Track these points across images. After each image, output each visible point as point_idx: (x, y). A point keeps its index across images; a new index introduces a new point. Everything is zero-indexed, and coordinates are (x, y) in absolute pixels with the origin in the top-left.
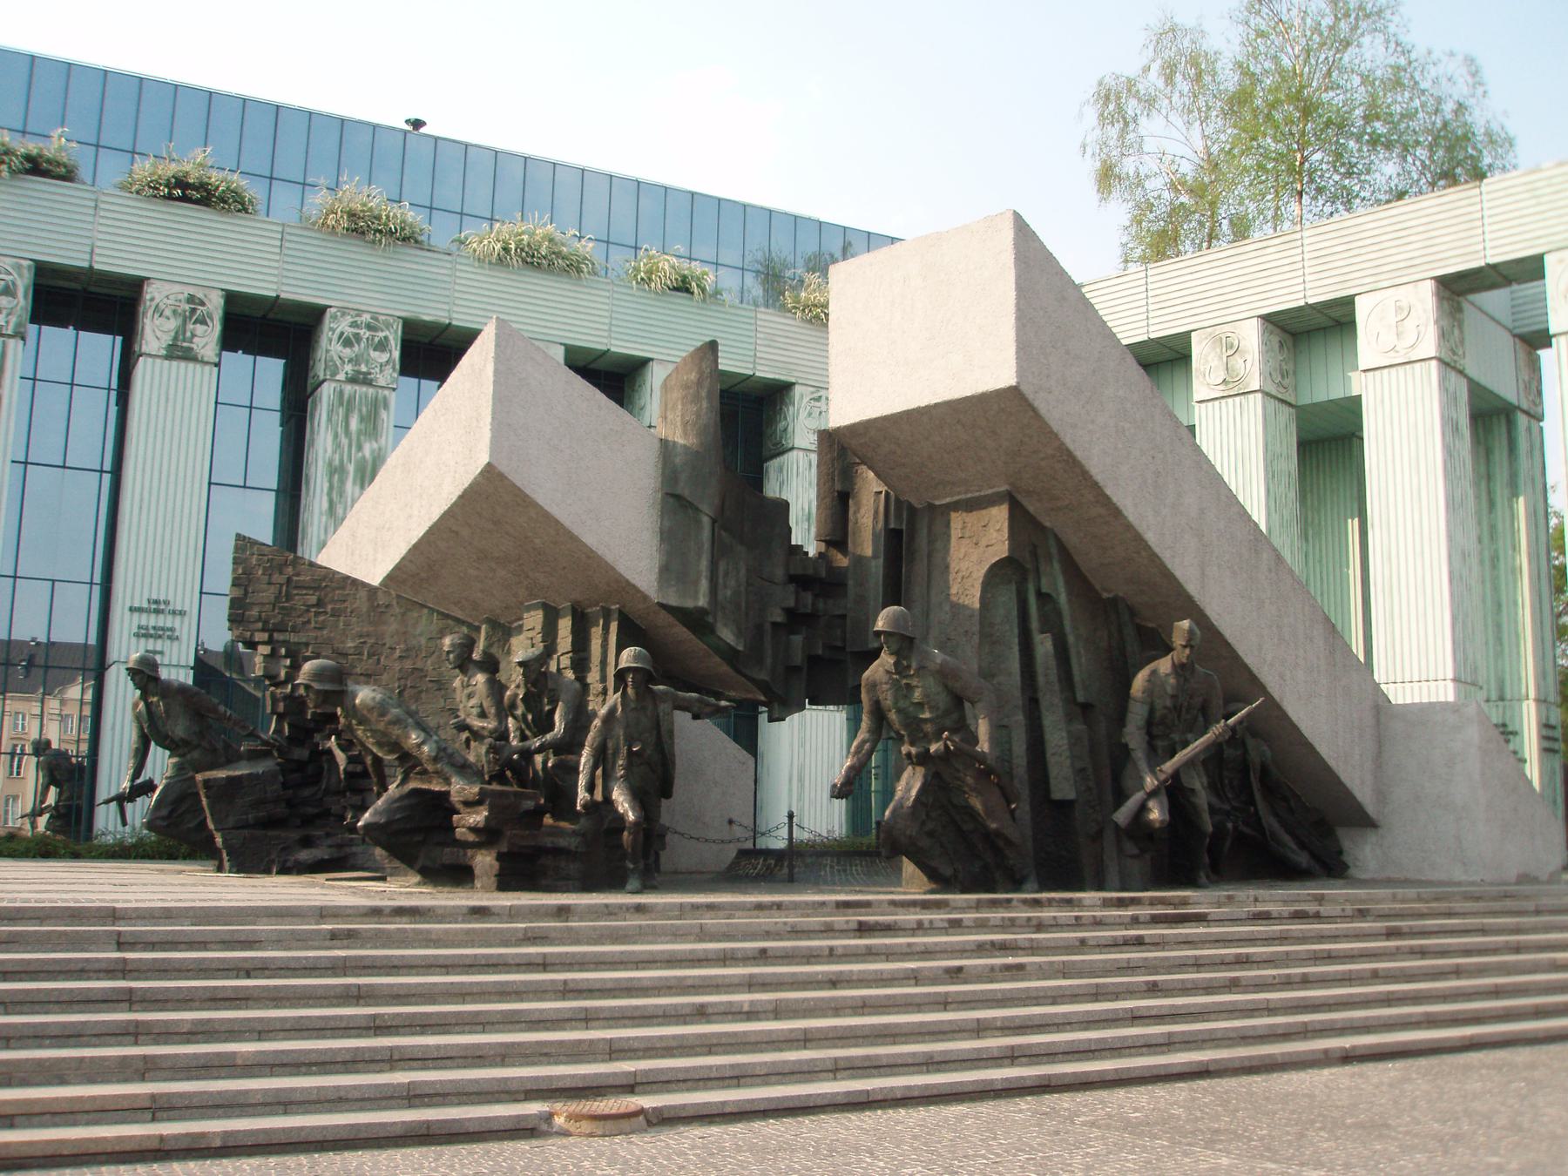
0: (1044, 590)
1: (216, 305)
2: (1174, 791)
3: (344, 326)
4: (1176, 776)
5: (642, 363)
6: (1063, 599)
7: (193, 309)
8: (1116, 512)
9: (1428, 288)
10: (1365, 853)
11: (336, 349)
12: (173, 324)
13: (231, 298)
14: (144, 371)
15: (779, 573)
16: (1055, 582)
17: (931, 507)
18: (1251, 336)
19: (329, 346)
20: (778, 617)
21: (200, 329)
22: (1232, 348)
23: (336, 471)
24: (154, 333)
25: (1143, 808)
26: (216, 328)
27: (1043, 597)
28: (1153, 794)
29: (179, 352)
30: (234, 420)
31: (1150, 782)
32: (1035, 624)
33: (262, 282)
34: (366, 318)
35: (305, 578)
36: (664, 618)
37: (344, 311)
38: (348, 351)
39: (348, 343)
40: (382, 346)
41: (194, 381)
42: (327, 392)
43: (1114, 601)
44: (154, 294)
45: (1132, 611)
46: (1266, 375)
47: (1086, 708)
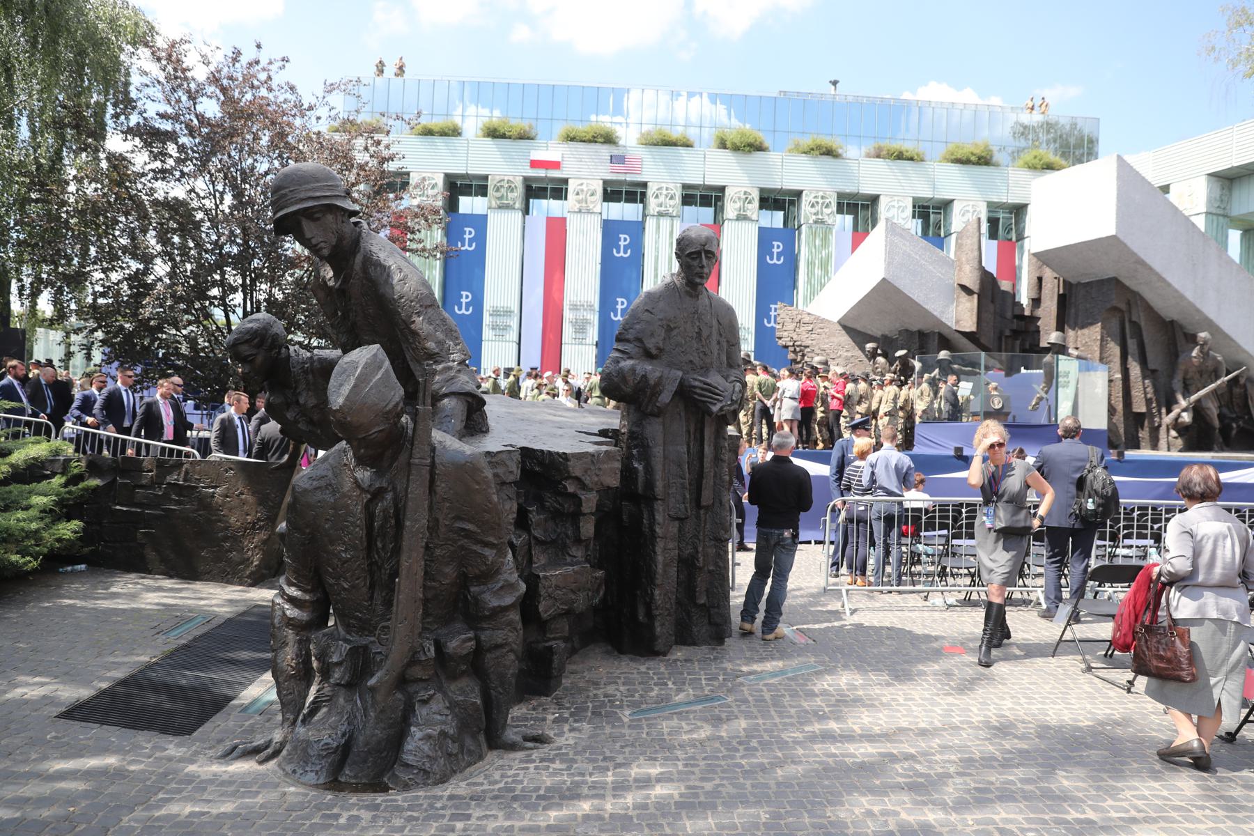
0: (1134, 319)
1: (756, 195)
2: (1197, 409)
3: (811, 198)
4: (1199, 401)
5: (952, 201)
6: (1143, 324)
8: (1169, 285)
11: (809, 209)
13: (762, 190)
15: (1009, 315)
17: (1079, 284)
19: (806, 210)
20: (1008, 333)
21: (750, 206)
23: (810, 264)
24: (730, 210)
25: (1179, 416)
26: (756, 203)
27: (1130, 321)
28: (1184, 410)
29: (742, 218)
31: (1183, 403)
32: (1128, 336)
34: (821, 194)
35: (807, 319)
36: (958, 335)
37: (811, 191)
38: (813, 210)
39: (813, 206)
43: (1172, 322)
45: (1181, 327)
47: (1153, 371)
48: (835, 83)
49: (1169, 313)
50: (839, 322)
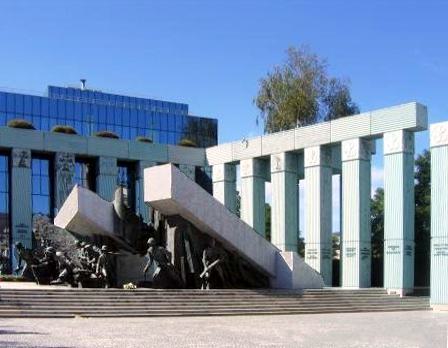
1: (29, 152)
4: (213, 267)
7: (24, 155)
9: (318, 148)
10: (273, 283)
12: (19, 160)
14: (14, 170)
16: (189, 230)
18: (282, 157)
22: (279, 159)
24: (16, 161)
29: (22, 165)
30: (37, 179)
33: (39, 147)
40: (71, 161)
41: (26, 172)
42: (58, 173)
44: (14, 151)
46: (286, 166)
48: (84, 81)
49: (204, 230)
50: (67, 228)
